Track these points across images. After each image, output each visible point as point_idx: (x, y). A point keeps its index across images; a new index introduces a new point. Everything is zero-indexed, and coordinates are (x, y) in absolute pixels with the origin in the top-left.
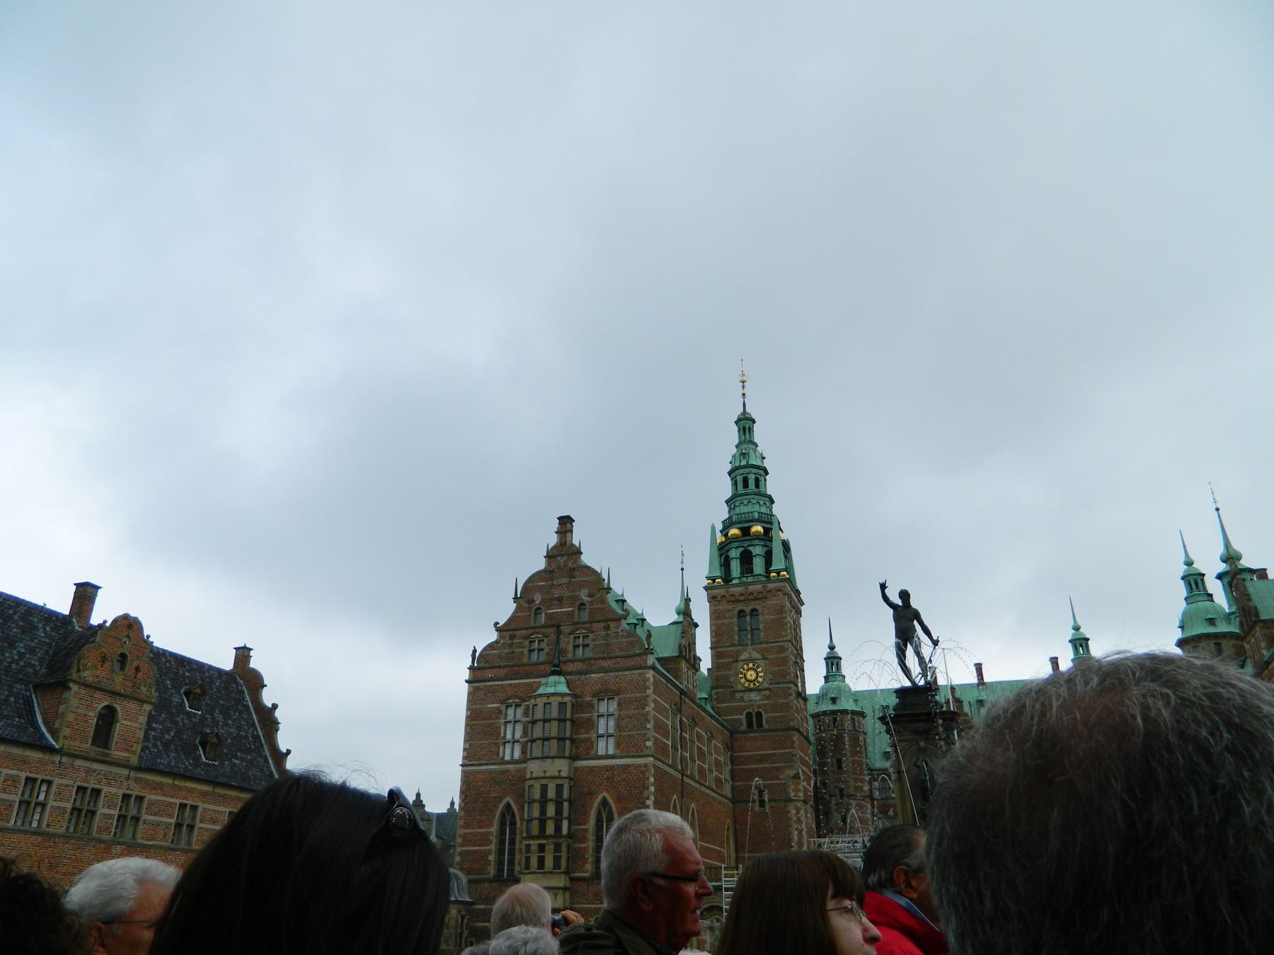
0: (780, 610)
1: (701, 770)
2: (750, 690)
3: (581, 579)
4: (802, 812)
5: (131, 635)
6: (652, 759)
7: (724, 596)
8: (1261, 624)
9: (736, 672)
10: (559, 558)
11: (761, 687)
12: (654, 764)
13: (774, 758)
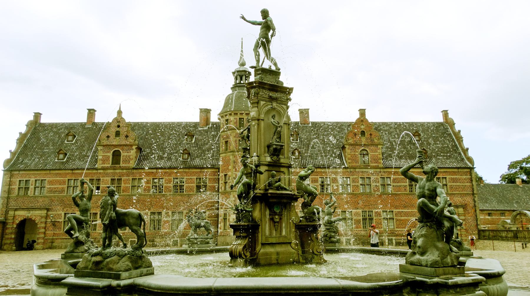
5: (363, 124)
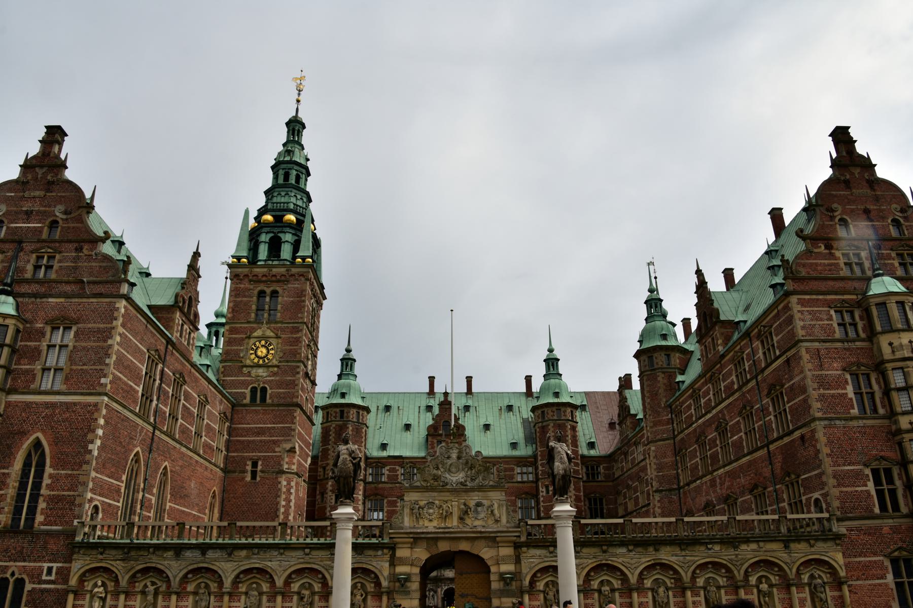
0: (301, 294)
1: (184, 430)
2: (258, 366)
3: (59, 194)
4: (293, 484)
6: (106, 399)
7: (246, 276)
8: (721, 324)
9: (247, 349)
10: (37, 169)
11: (269, 364)
12: (106, 405)
13: (273, 431)
